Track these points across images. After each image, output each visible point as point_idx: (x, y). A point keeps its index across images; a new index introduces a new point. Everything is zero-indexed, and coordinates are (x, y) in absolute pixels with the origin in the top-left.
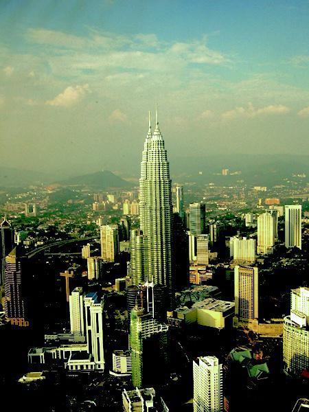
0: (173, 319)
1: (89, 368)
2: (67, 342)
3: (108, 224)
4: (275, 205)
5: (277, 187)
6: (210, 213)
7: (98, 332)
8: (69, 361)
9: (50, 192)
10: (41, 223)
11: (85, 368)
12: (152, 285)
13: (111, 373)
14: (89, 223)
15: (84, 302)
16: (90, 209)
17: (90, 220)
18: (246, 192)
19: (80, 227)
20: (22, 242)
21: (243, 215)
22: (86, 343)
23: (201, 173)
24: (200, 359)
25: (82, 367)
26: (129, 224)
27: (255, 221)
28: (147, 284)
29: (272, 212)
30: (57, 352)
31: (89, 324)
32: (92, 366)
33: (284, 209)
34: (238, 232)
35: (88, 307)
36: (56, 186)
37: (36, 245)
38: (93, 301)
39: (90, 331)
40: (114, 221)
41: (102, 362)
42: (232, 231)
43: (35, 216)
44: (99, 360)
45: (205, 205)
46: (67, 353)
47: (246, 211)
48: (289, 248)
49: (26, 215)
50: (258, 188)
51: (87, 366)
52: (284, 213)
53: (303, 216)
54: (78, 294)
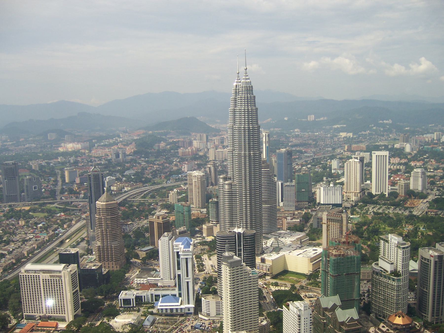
0: (262, 264)
1: (179, 311)
2: (155, 285)
3: (194, 170)
4: (361, 151)
5: (364, 133)
6: (295, 159)
7: (187, 276)
8: (160, 304)
9: (135, 138)
10: (128, 169)
11: (175, 311)
12: (240, 230)
13: (200, 316)
14: (175, 168)
15: (173, 246)
16: (176, 155)
17: (176, 165)
18: (332, 138)
19: (166, 173)
20: (110, 187)
21: (329, 161)
22: (175, 286)
23: (286, 119)
24: (290, 303)
25: (172, 310)
26: (215, 170)
27: (342, 167)
28: (237, 230)
29: (358, 158)
30: (147, 295)
31: (179, 269)
32: (181, 309)
33: (371, 156)
34: (325, 178)
35: (178, 253)
36: (142, 131)
37: (123, 191)
38: (183, 246)
39: (179, 276)
40: (199, 167)
41: (192, 305)
42: (318, 179)
43: (122, 161)
44: (189, 303)
45: (291, 151)
46: (157, 297)
47: (332, 157)
48: (376, 195)
49: (113, 160)
50: (343, 134)
51: (177, 309)
52: (371, 159)
53: (389, 163)
54: (167, 239)
